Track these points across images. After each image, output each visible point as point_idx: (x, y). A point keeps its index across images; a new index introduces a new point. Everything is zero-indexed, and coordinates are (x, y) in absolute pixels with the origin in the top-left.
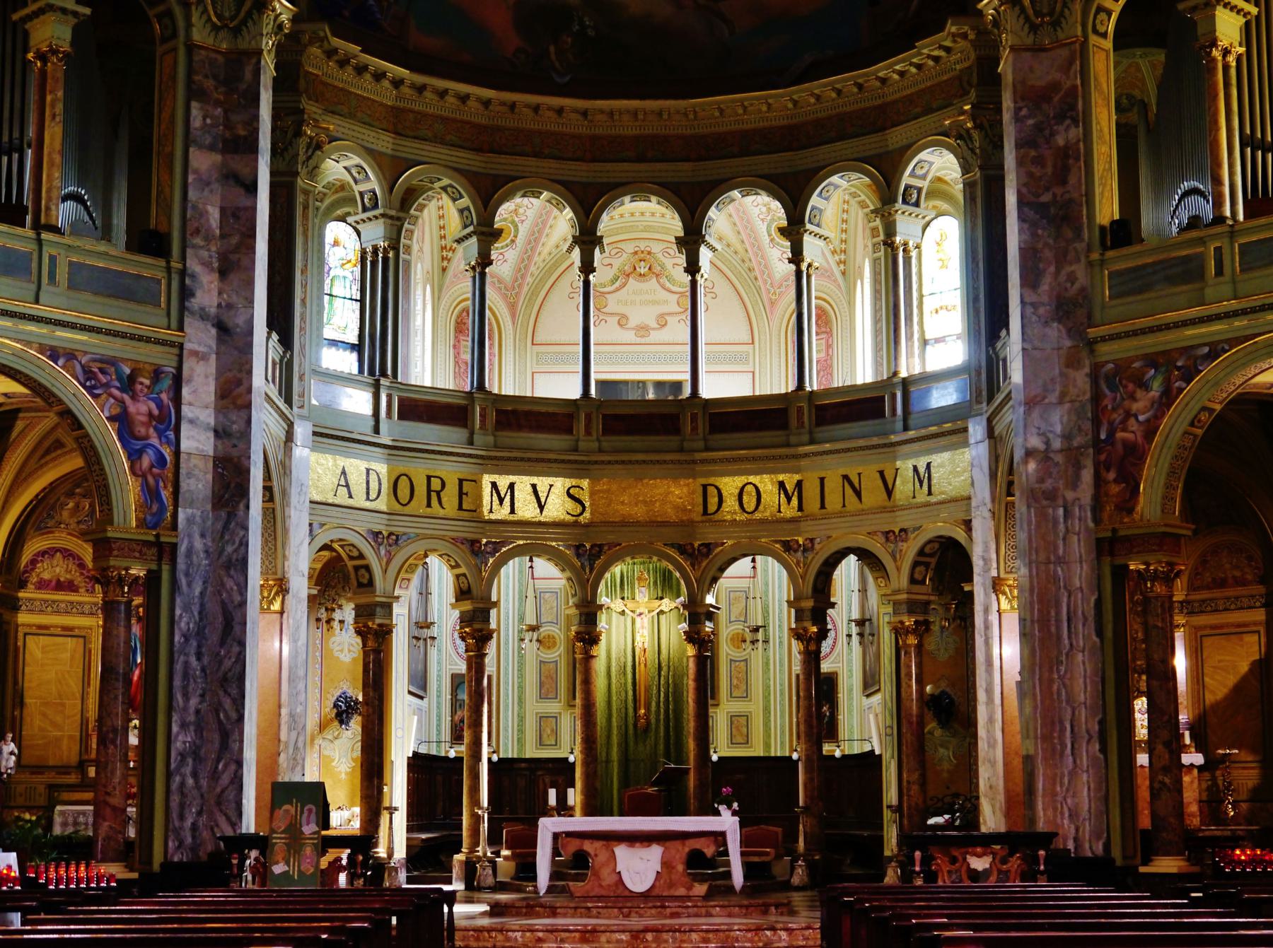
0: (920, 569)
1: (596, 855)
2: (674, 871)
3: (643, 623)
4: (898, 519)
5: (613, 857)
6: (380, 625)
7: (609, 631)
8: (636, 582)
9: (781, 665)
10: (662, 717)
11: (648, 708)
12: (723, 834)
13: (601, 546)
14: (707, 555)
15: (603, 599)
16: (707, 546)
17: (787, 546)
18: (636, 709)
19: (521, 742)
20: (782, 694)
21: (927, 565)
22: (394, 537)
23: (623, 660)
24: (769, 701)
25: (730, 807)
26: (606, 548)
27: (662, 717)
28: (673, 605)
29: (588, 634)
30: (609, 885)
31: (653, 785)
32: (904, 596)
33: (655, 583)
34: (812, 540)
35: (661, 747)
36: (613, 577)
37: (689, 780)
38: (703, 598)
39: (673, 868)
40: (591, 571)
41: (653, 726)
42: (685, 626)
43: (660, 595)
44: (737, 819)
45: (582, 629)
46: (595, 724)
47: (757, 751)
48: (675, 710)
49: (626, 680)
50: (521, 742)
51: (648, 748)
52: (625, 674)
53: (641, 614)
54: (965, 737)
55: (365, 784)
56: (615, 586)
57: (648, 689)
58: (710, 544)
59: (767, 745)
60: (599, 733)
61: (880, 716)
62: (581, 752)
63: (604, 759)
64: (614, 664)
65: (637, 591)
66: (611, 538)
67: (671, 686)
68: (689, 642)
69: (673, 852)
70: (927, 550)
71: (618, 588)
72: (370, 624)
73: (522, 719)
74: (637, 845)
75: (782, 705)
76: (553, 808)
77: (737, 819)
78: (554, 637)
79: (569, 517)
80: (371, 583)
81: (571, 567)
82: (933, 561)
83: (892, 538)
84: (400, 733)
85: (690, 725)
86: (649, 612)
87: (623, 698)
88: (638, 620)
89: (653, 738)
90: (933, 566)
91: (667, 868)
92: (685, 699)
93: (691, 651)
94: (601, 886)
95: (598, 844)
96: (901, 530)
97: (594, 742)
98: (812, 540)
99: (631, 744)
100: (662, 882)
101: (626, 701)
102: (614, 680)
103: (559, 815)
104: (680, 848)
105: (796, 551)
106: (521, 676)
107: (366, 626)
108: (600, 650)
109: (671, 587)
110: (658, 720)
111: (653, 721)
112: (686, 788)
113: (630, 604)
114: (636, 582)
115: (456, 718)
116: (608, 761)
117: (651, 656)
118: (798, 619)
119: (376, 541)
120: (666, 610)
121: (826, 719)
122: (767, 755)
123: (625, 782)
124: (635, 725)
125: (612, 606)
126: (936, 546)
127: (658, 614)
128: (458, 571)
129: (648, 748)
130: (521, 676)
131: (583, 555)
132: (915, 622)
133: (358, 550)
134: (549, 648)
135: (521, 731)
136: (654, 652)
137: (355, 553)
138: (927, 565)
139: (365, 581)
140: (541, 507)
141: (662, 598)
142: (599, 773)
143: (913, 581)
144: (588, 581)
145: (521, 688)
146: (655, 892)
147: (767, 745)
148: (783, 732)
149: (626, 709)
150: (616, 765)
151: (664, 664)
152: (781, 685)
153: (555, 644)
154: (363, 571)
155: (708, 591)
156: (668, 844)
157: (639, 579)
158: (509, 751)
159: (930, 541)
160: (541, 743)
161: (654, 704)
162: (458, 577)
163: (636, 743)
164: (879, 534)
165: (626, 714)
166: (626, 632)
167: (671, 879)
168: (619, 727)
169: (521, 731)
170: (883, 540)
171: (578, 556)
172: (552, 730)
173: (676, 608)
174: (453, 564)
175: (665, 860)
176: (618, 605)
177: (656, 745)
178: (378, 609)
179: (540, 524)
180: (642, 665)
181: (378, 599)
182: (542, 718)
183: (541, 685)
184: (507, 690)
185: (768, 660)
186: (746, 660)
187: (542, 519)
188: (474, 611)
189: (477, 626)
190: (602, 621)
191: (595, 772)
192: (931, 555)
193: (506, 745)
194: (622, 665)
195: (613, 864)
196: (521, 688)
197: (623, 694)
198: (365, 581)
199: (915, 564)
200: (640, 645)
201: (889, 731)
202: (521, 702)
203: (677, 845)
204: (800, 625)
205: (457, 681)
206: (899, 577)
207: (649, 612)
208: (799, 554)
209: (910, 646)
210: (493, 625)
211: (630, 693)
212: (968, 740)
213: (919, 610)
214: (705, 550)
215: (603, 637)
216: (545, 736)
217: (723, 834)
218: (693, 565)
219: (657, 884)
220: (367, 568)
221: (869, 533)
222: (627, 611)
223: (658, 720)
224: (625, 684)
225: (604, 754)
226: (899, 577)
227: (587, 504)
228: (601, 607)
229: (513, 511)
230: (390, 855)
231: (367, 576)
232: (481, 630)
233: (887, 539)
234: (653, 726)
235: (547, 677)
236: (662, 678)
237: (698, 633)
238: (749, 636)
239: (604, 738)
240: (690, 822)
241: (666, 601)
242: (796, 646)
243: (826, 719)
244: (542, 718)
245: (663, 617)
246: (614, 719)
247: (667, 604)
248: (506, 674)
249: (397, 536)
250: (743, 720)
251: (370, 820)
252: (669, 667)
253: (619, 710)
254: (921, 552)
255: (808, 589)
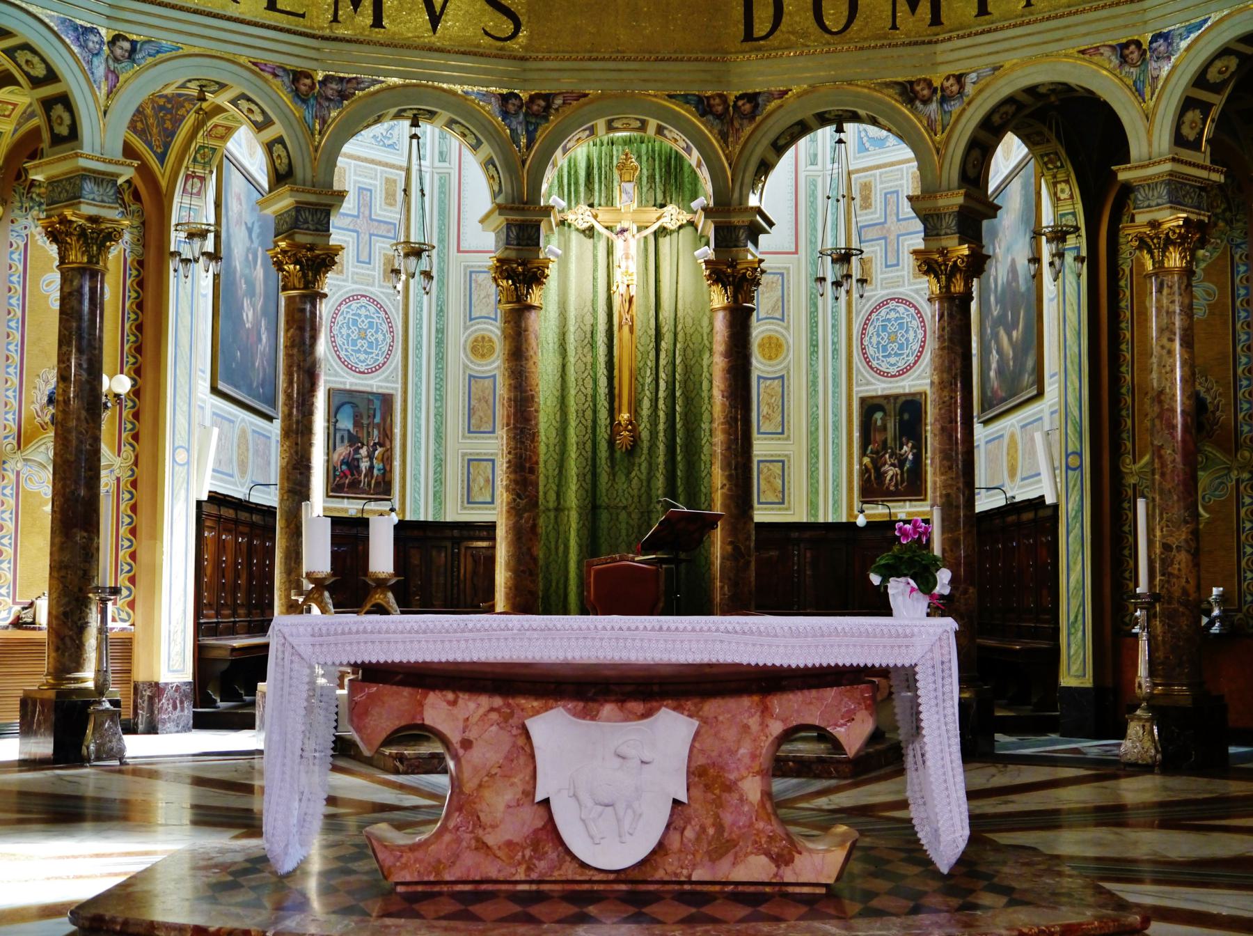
0: (1193, 115)
1: (467, 744)
2: (734, 798)
3: (627, 248)
4: (1150, 15)
5: (525, 748)
6: (93, 219)
7: (564, 261)
8: (615, 171)
9: (836, 384)
10: (661, 427)
11: (635, 409)
12: (908, 676)
13: (548, 98)
14: (752, 117)
15: (550, 194)
16: (752, 98)
17: (908, 93)
18: (612, 412)
19: (439, 498)
20: (836, 428)
21: (1205, 108)
22: (127, 45)
23: (589, 320)
24: (816, 439)
25: (925, 583)
26: (559, 101)
27: (661, 427)
28: (685, 217)
29: (523, 264)
30: (509, 844)
31: (647, 548)
32: (1168, 167)
33: (652, 178)
34: (959, 78)
35: (660, 482)
36: (572, 166)
37: (712, 544)
38: (743, 198)
39: (729, 787)
40: (529, 146)
41: (645, 445)
42: (708, 252)
43: (660, 200)
44: (949, 624)
45: (512, 254)
46: (534, 436)
47: (798, 515)
48: (686, 415)
49: (595, 357)
50: (439, 498)
51: (635, 481)
52: (593, 345)
53: (623, 231)
54: (1229, 469)
55: (57, 540)
56: (576, 183)
57: (635, 376)
58: (756, 95)
59: (813, 506)
60: (542, 458)
61: (1056, 436)
62: (507, 489)
63: (551, 505)
64: (572, 328)
65: (616, 193)
66: (567, 83)
67: (679, 369)
68: (716, 282)
69: (730, 734)
70: (1213, 75)
71: (582, 189)
72: (68, 213)
73: (440, 463)
74: (608, 709)
75: (836, 445)
76: (381, 583)
77: (949, 624)
78: (490, 340)
79: (486, 41)
80: (74, 133)
81: (493, 135)
82: (1218, 101)
83: (1135, 56)
84: (181, 456)
85: (715, 441)
86: (640, 229)
87: (590, 391)
88: (619, 243)
89: (644, 466)
90: (1215, 113)
91: (708, 788)
92: (705, 394)
93: (718, 298)
94: (482, 846)
95: (474, 706)
96: (1155, 38)
97: (532, 471)
98: (959, 78)
99: (604, 478)
100: (689, 833)
101: (594, 397)
102: (572, 359)
103: (407, 606)
104: (754, 722)
105: (926, 102)
106: (441, 398)
107: (64, 221)
108: (545, 297)
109: (680, 188)
110: (653, 434)
111: (645, 435)
112: (709, 563)
113: (604, 215)
114: (615, 171)
115: (336, 457)
116: (559, 509)
117: (642, 314)
118: (930, 233)
119: (83, 46)
120: (672, 226)
121: (907, 465)
122: (812, 520)
123: (591, 547)
124: (611, 443)
125: (570, 217)
126: (1233, 63)
127: (656, 234)
128: (270, 133)
129: (635, 481)
130: (441, 398)
131: (516, 114)
132: (1186, 220)
133: (43, 60)
134: (483, 356)
135: (440, 481)
136: (647, 307)
137: (40, 71)
138: (1205, 108)
139: (64, 131)
140: (435, 20)
141: (662, 206)
142: (541, 530)
143: (1179, 140)
144: (524, 162)
145: (440, 416)
146: (668, 869)
147: (813, 506)
148: (837, 487)
149: (595, 412)
150: (574, 516)
151: (666, 329)
152: (835, 415)
153: (492, 350)
154: (59, 110)
155: (753, 187)
156: (712, 707)
157: (622, 167)
158: (421, 512)
159: (1225, 52)
160: (470, 501)
161: (646, 404)
162: (269, 147)
163: (613, 474)
164: (1107, 52)
165: (595, 421)
166: (595, 270)
167: (720, 827)
168: (581, 445)
169: (440, 481)
170: (1116, 61)
171: (505, 114)
172: (487, 481)
173: (691, 223)
174: (259, 118)
175: (701, 760)
176: (580, 216)
177: (649, 481)
178: (88, 186)
179: (431, 49)
180: (626, 329)
181: (83, 163)
182: (471, 462)
183: (471, 412)
184: (419, 418)
185: (816, 377)
186: (782, 377)
187: (435, 40)
188: (299, 208)
189: (302, 238)
190: (550, 245)
191: (534, 527)
192: (1216, 88)
193: (416, 501)
194: (588, 328)
195: (529, 770)
196: (440, 416)
197: (589, 384)
198: (64, 131)
199: (1188, 104)
200: (622, 289)
201: (1073, 461)
202: (440, 436)
203: (743, 709)
204: (934, 245)
205: (336, 401)
206: (1149, 132)
207: (640, 229)
208: (934, 106)
209: (1170, 271)
210: (336, 238)
211: (603, 382)
212: (1234, 475)
213: (1188, 200)
214: (747, 107)
215: (552, 271)
216: (475, 489)
217: (908, 676)
218: (724, 137)
219: (675, 841)
220: (65, 100)
221: (1083, 52)
222: (598, 227)
223: (653, 434)
224: (594, 365)
225: (552, 496)
226: (1149, 132)
227: (523, 19)
228: (547, 210)
229: (378, 22)
230: (101, 689)
231: (66, 117)
232: (312, 248)
233: (1124, 60)
234: (645, 445)
235: (479, 400)
236: (663, 355)
237: (733, 264)
238: (830, 271)
239: (552, 465)
240: (794, 633)
241: (671, 209)
242: (922, 288)
243: (907, 465)
244: (471, 462)
245: (665, 242)
246: (572, 432)
247: (673, 215)
248: (417, 394)
249: (134, 43)
250: (777, 468)
251: (65, 614)
252: (675, 335)
253: (581, 414)
254: (1200, 80)
255: (952, 172)
